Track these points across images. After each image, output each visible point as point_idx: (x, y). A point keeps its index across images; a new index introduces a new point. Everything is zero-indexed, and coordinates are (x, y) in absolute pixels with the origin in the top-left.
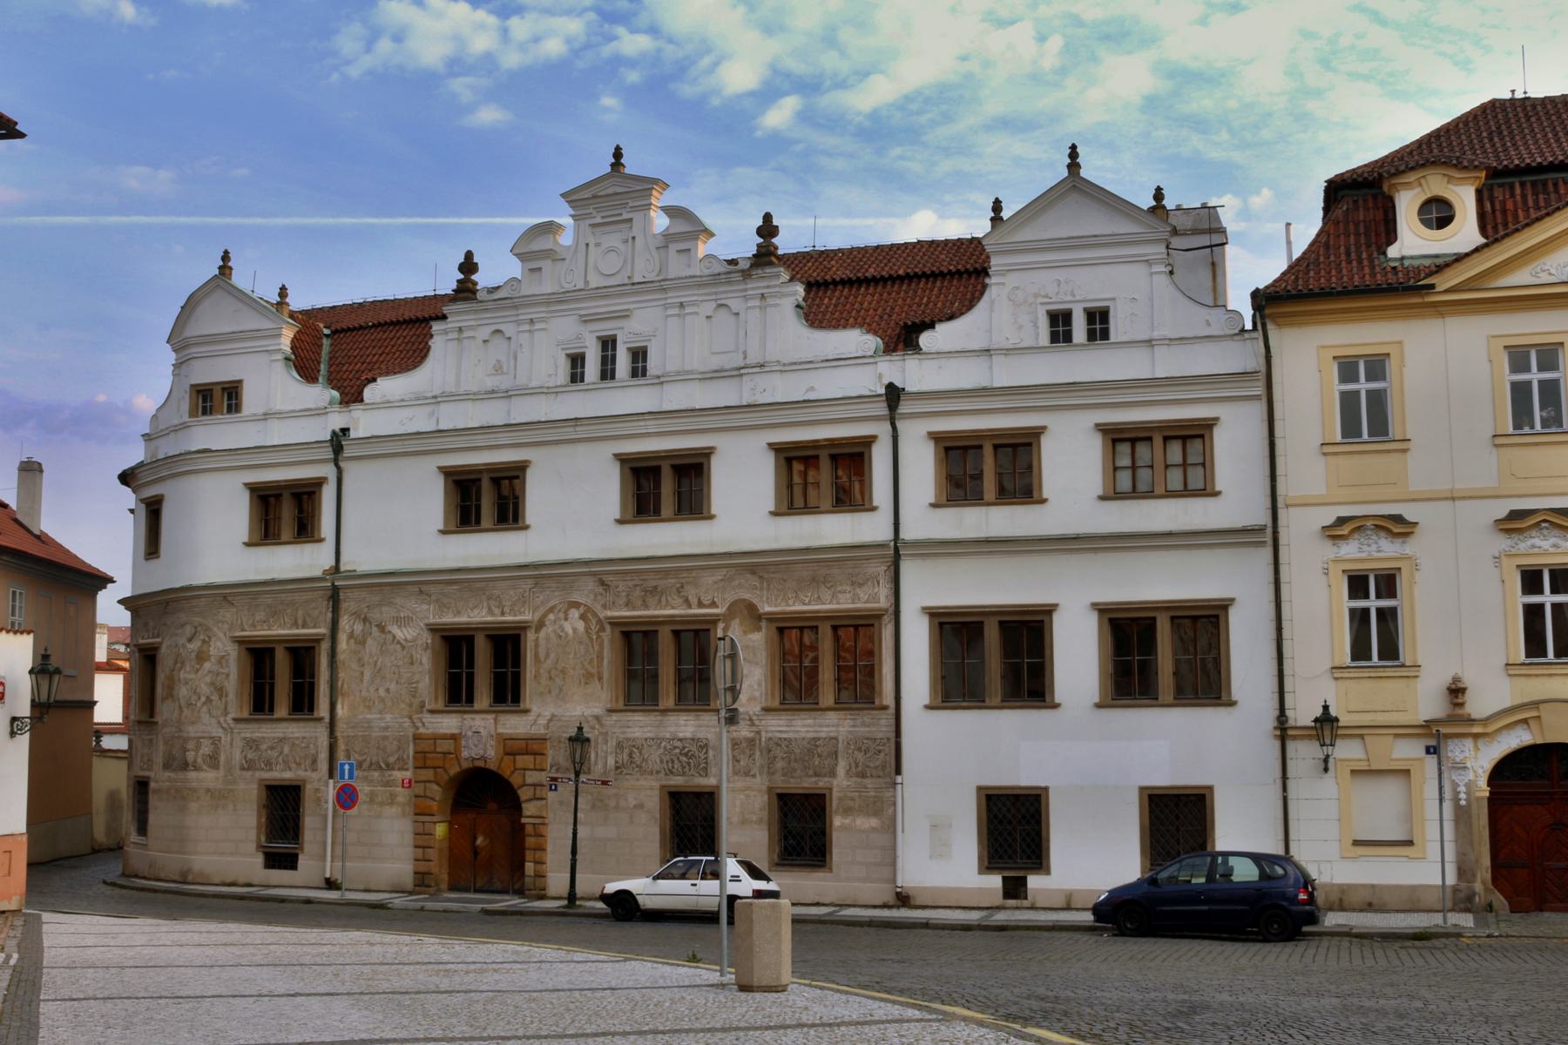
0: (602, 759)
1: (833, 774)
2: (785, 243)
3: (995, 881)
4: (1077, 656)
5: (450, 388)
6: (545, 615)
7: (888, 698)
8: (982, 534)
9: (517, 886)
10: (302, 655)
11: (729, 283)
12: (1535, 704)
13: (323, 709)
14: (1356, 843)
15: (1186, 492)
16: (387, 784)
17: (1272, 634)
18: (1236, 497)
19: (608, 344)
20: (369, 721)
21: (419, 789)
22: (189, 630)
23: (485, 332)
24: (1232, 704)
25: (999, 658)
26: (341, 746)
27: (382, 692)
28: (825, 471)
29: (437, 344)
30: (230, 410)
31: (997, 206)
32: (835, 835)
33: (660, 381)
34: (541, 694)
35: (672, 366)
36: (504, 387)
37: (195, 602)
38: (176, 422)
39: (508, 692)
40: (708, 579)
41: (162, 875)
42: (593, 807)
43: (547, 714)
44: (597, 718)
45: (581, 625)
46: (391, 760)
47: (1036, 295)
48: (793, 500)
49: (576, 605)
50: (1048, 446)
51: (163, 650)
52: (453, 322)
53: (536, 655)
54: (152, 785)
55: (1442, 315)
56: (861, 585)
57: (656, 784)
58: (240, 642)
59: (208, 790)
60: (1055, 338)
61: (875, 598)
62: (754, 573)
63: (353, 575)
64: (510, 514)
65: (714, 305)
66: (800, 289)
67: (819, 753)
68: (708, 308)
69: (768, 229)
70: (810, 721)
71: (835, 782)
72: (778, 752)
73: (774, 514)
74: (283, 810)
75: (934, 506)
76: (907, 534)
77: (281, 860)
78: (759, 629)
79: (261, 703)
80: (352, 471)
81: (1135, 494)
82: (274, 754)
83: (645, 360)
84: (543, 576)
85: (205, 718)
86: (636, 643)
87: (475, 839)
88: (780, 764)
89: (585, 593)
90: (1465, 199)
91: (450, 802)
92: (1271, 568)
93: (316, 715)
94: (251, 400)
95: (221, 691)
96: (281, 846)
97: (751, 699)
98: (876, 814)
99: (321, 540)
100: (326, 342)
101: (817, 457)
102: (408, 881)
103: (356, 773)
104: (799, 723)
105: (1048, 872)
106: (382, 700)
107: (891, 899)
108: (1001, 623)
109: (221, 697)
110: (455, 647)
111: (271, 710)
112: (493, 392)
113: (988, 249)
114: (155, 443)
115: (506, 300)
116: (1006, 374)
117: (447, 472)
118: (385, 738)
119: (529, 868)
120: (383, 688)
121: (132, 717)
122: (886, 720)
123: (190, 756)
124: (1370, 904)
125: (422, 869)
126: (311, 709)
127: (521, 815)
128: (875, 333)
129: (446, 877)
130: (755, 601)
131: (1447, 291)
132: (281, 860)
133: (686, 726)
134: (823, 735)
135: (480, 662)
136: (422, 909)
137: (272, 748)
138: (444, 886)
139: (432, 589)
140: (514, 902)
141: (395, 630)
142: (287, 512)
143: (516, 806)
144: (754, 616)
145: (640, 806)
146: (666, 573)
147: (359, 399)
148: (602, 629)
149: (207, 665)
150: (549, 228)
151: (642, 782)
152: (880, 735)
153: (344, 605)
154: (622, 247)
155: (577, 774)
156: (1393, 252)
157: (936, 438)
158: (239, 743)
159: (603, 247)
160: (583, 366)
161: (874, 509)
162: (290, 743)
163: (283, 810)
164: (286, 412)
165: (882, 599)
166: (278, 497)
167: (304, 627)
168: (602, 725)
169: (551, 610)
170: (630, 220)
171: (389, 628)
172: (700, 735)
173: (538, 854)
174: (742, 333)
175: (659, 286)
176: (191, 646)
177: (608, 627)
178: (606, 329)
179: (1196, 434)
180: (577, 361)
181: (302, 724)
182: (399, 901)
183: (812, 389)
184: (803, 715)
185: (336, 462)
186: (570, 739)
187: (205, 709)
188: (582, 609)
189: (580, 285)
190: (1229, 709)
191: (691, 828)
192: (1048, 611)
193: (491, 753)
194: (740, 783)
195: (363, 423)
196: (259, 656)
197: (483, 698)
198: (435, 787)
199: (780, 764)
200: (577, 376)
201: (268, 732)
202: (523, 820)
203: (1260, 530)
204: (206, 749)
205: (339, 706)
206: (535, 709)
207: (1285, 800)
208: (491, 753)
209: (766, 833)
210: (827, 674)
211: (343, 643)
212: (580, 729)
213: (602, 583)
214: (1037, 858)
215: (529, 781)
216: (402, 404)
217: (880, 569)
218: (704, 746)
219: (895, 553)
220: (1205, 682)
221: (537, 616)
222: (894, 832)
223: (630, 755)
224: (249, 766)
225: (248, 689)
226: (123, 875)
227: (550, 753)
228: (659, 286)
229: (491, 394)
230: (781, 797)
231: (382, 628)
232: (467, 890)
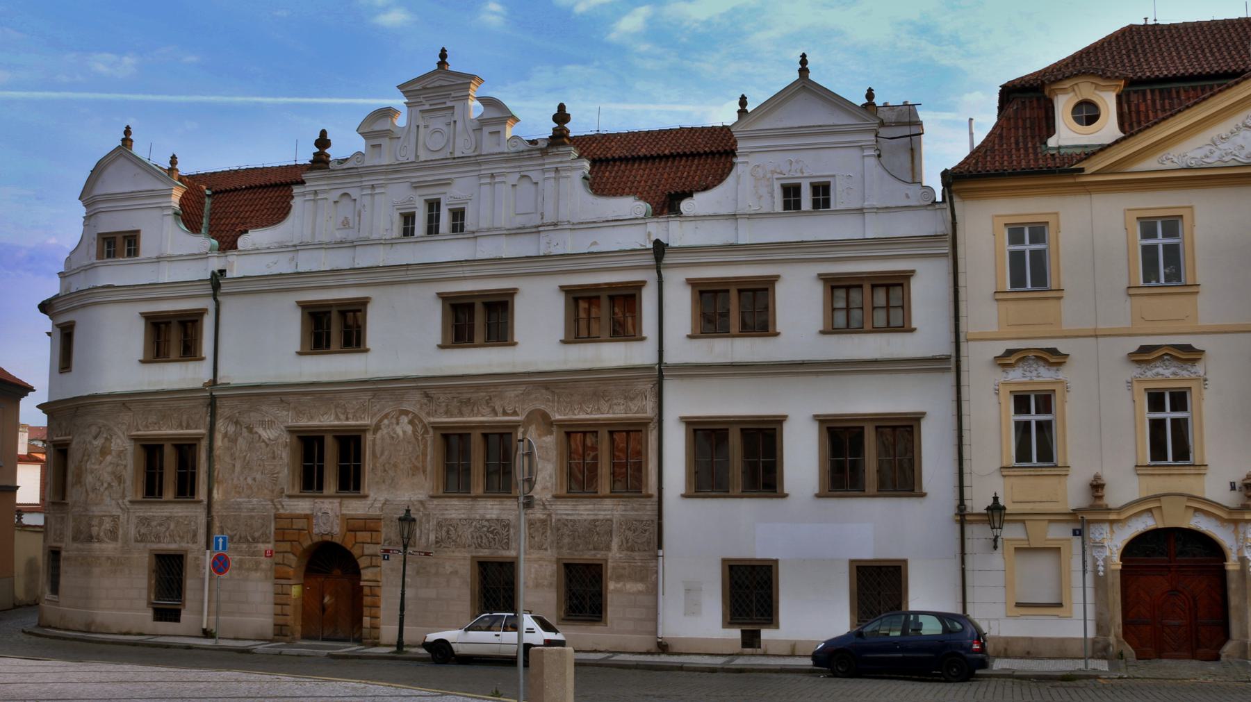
0: (426, 535)
1: (608, 548)
2: (576, 128)
3: (735, 634)
4: (802, 458)
5: (308, 239)
6: (381, 421)
7: (652, 489)
8: (728, 360)
9: (356, 636)
10: (186, 451)
11: (531, 158)
12: (1158, 497)
13: (202, 494)
14: (1018, 605)
15: (889, 328)
16: (254, 554)
17: (955, 441)
18: (927, 333)
19: (433, 205)
20: (240, 503)
21: (279, 558)
23: (335, 195)
24: (923, 495)
25: (740, 458)
26: (217, 524)
27: (249, 481)
28: (604, 309)
29: (297, 203)
30: (129, 255)
31: (743, 101)
32: (609, 596)
33: (474, 235)
35: (484, 224)
36: (350, 239)
38: (86, 263)
39: (351, 481)
40: (511, 393)
41: (71, 626)
42: (418, 573)
43: (382, 499)
44: (421, 502)
45: (409, 429)
46: (257, 534)
47: (773, 172)
48: (577, 332)
49: (406, 413)
50: (780, 290)
51: (74, 445)
52: (310, 187)
54: (63, 554)
55: (1089, 193)
56: (632, 399)
57: (468, 555)
58: (136, 439)
59: (109, 558)
60: (787, 206)
61: (643, 410)
62: (547, 389)
63: (227, 387)
64: (353, 340)
65: (518, 176)
66: (587, 165)
67: (596, 531)
68: (514, 178)
69: (561, 116)
70: (590, 507)
71: (610, 555)
72: (565, 531)
73: (564, 342)
74: (169, 574)
75: (689, 337)
76: (669, 359)
77: (168, 614)
78: (551, 433)
79: (152, 488)
80: (228, 305)
81: (848, 329)
82: (163, 529)
83: (463, 218)
84: (380, 389)
85: (107, 500)
86: (453, 442)
87: (323, 598)
88: (566, 540)
89: (413, 403)
90: (1108, 102)
91: (303, 569)
92: (954, 389)
93: (196, 498)
94: (147, 247)
95: (120, 479)
96: (168, 603)
97: (544, 488)
98: (642, 580)
99: (202, 359)
100: (207, 200)
101: (598, 298)
102: (270, 632)
103: (228, 545)
104: (582, 507)
105: (777, 627)
106: (250, 487)
107: (653, 647)
108: (742, 430)
110: (309, 445)
111: (160, 494)
112: (341, 242)
113: (736, 135)
114: (68, 280)
115: (352, 170)
116: (748, 234)
117: (304, 306)
118: (252, 517)
119: (366, 621)
120: (251, 478)
121: (48, 499)
122: (651, 506)
123: (95, 530)
124: (1028, 653)
125: (281, 622)
126: (193, 494)
127: (360, 580)
128: (646, 200)
129: (299, 628)
130: (548, 411)
131: (1093, 174)
132: (168, 614)
133: (492, 509)
134: (601, 517)
135: (329, 458)
136: (280, 653)
137: (160, 525)
138: (298, 635)
139: (291, 399)
140: (353, 648)
141: (261, 431)
142: (175, 336)
143: (356, 571)
144: (548, 423)
145: (455, 573)
146: (478, 388)
147: (233, 246)
148: (426, 432)
149: (109, 458)
150: (387, 112)
151: (456, 554)
152: (646, 518)
153: (219, 411)
154: (445, 129)
155: (405, 547)
156: (1052, 142)
157: (692, 283)
158: (134, 521)
159: (431, 128)
160: (413, 223)
161: (643, 339)
162: (176, 521)
163: (169, 574)
164: (176, 256)
165: (649, 411)
166: (168, 324)
169: (386, 416)
170: (453, 107)
171: (256, 429)
172: (504, 517)
173: (374, 611)
174: (540, 199)
175: (475, 160)
176: (95, 443)
177: (431, 431)
178: (432, 193)
179: (897, 283)
180: (408, 219)
181: (185, 506)
182: (261, 647)
183: (595, 243)
184: (586, 501)
185: (215, 299)
186: (400, 519)
187: (107, 493)
188: (410, 416)
189: (412, 159)
190: (921, 499)
191: (495, 590)
192: (779, 421)
193: (336, 529)
194: (535, 555)
195: (237, 265)
196: (151, 451)
197: (331, 485)
198: (291, 556)
199: (566, 540)
200: (408, 231)
201: (157, 511)
202: (362, 583)
203: (945, 359)
204: (108, 525)
205: (215, 491)
206: (372, 495)
207: (963, 571)
208: (336, 529)
209: (555, 595)
210: (604, 469)
211: (219, 442)
212: (408, 511)
213: (427, 395)
214: (769, 616)
215: (366, 552)
216: (268, 251)
217: (648, 387)
218: (506, 526)
219: (659, 374)
220: (902, 479)
221: (375, 421)
222: (656, 595)
223: (448, 532)
224: (142, 539)
225: (142, 478)
226: (39, 626)
227: (384, 530)
228: (475, 160)
229: (341, 244)
230: (567, 566)
231: (250, 430)
232: (316, 639)
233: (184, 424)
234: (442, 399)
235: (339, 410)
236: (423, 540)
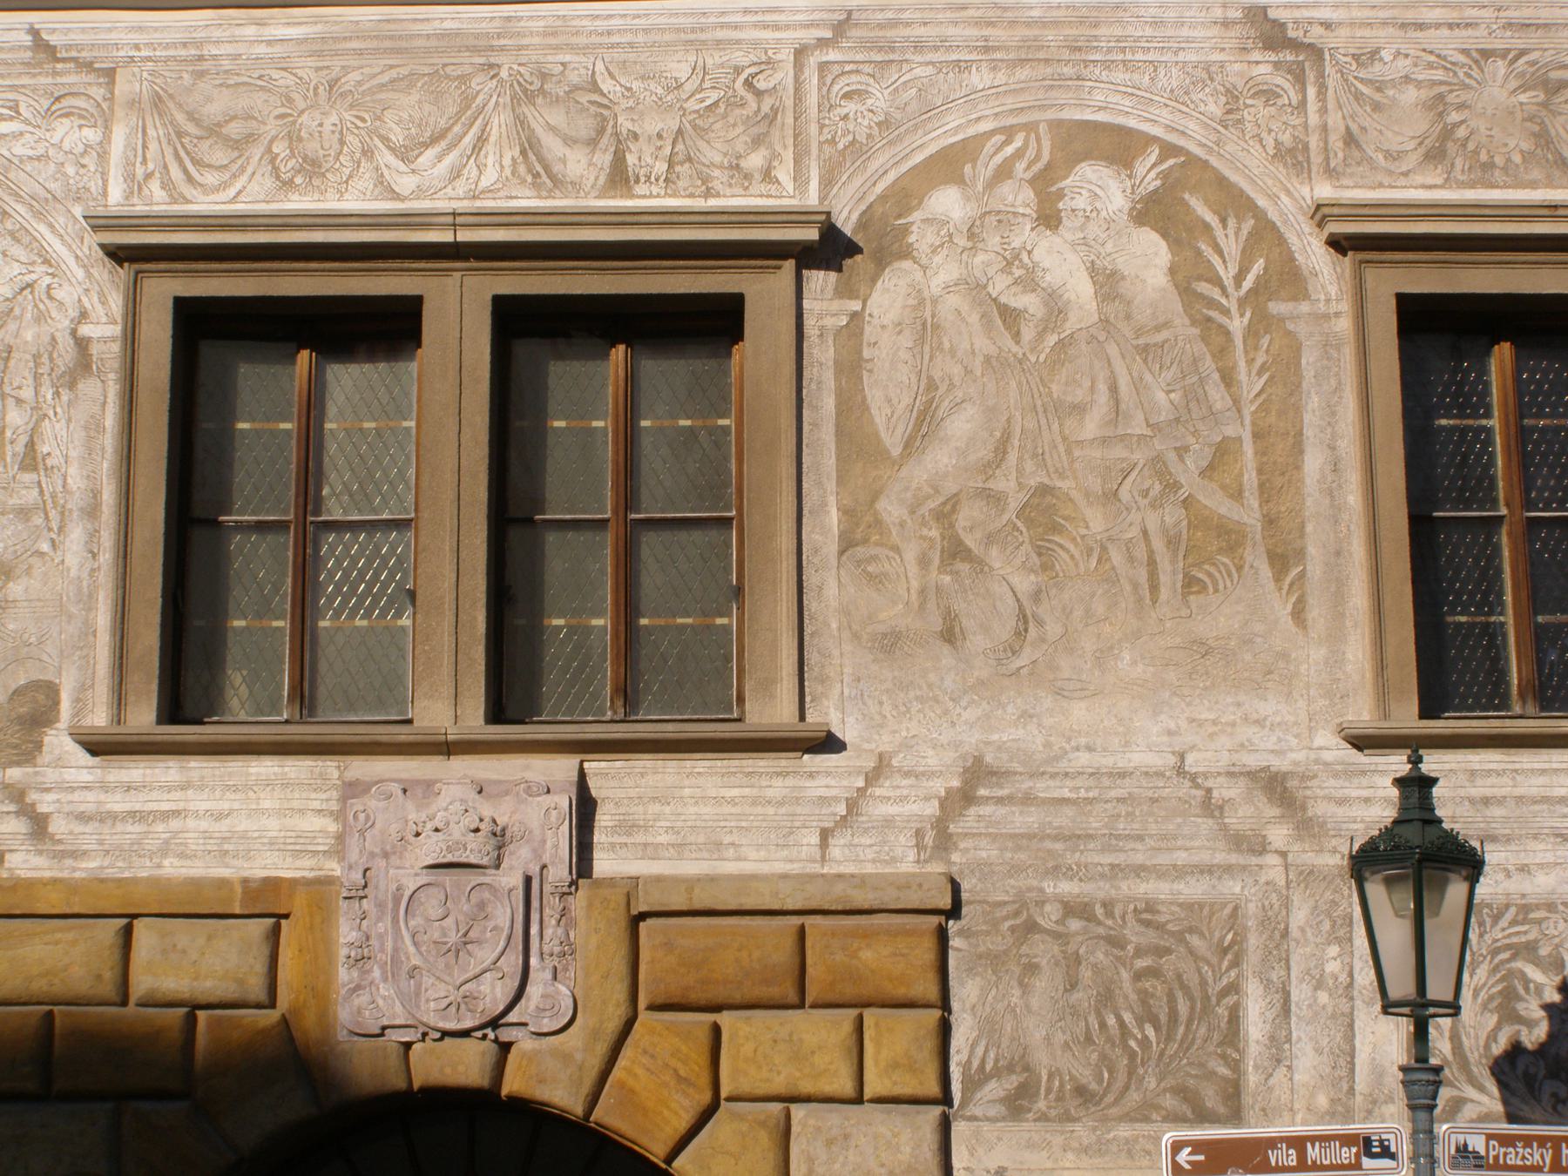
6: (906, 195)
34: (889, 644)
44: (1277, 787)
45: (1148, 259)
49: (1119, 146)
53: (851, 406)
168: (1307, 827)
169: (948, 165)
177: (1326, 272)
234: (1390, 67)
235: (545, 119)
236: (1307, 1062)
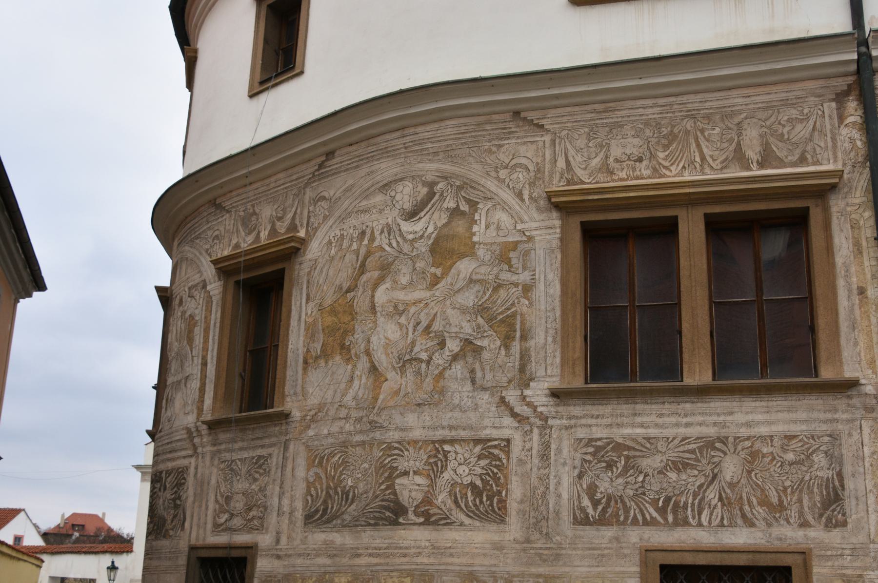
22: (406, 194)
37: (425, 132)
51: (314, 250)
58: (562, 205)
82: (692, 479)
85: (459, 390)
95: (509, 328)
109: (507, 341)
123: (410, 489)
137: (680, 466)
149: (465, 267)
158: (566, 452)
167: (761, 165)
181: (779, 402)
187: (458, 369)
204: (463, 468)
224: (604, 513)
233: (753, 154)
